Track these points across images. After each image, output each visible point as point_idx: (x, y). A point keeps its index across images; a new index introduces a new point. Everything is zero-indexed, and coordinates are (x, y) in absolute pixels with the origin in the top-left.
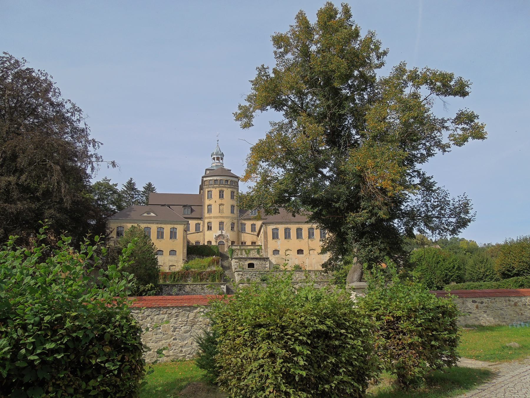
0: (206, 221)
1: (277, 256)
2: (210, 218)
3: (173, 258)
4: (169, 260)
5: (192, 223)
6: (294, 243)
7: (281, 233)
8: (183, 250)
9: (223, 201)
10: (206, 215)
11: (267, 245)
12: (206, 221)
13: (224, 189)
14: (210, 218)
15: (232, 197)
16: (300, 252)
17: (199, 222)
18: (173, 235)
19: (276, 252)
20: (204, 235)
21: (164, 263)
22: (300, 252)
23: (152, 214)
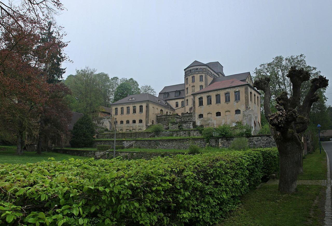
0: (186, 99)
1: (202, 119)
2: (187, 96)
3: (141, 124)
4: (139, 126)
5: (180, 101)
6: (215, 108)
7: (205, 101)
8: (146, 119)
9: (194, 84)
10: (186, 95)
11: (195, 111)
12: (186, 99)
13: (195, 75)
14: (187, 96)
15: (201, 80)
16: (218, 114)
17: (183, 100)
18: (141, 110)
19: (201, 116)
20: (185, 108)
21: (136, 128)
22: (218, 114)
23: (134, 99)
